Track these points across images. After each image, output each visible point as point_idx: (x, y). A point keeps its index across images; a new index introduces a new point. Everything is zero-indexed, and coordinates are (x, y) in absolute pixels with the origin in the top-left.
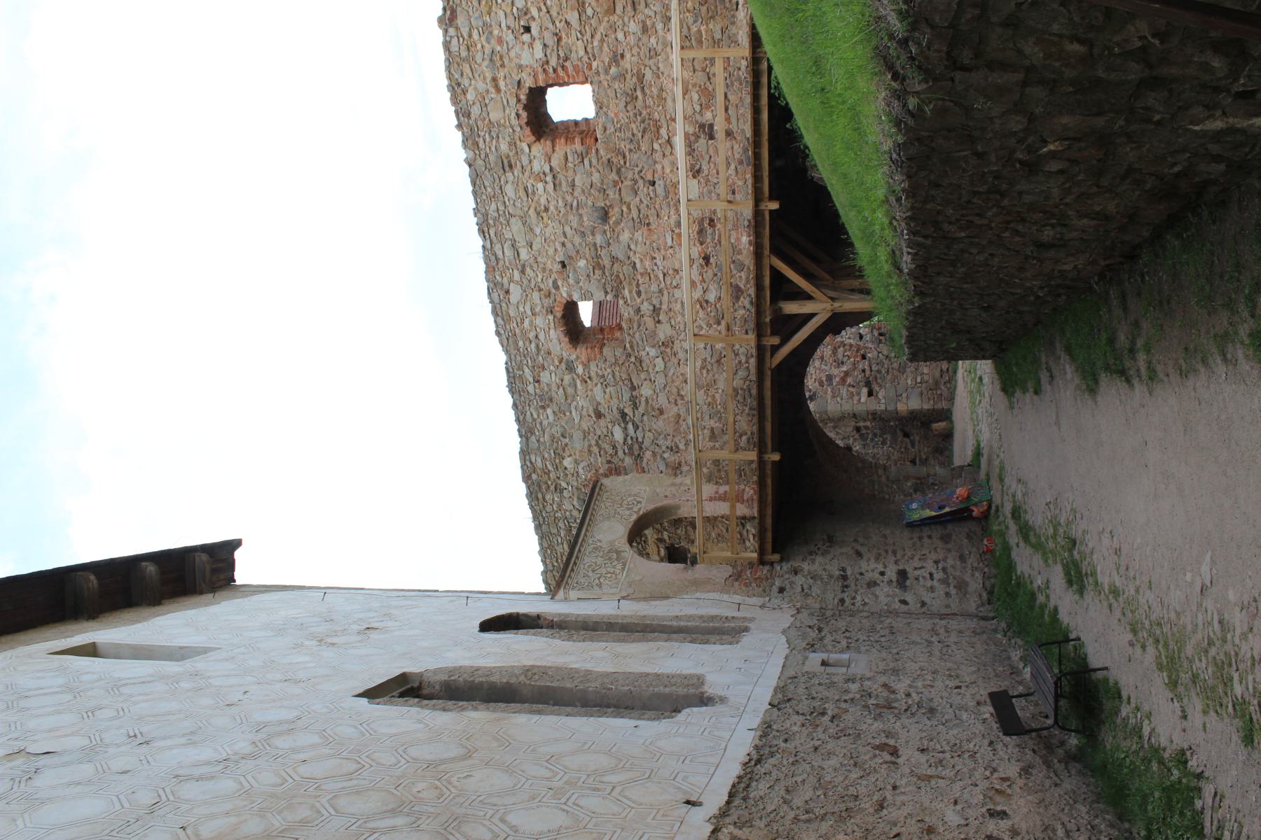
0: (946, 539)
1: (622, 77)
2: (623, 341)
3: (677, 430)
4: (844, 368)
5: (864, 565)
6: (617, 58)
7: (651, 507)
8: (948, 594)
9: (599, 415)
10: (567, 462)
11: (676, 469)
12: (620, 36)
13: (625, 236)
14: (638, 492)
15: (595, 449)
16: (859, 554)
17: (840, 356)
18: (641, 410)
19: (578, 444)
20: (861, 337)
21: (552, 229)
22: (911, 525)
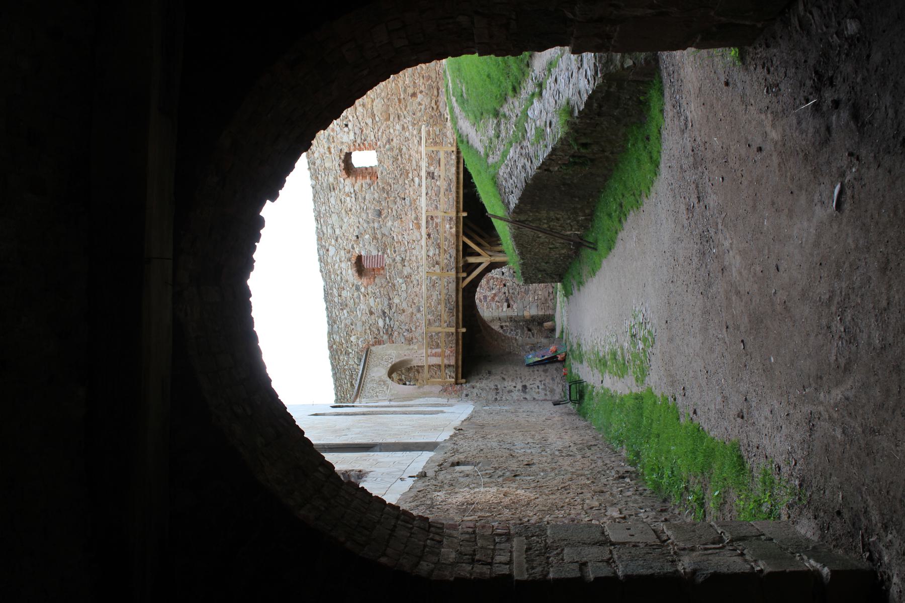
0: (545, 371)
1: (392, 149)
2: (385, 275)
3: (411, 320)
4: (494, 292)
5: (506, 384)
6: (389, 141)
7: (398, 360)
8: (546, 395)
9: (371, 313)
10: (353, 339)
11: (410, 341)
12: (392, 131)
13: (390, 223)
14: (390, 353)
15: (368, 331)
16: (504, 379)
17: (491, 285)
18: (393, 310)
19: (359, 328)
20: (503, 274)
21: (353, 219)
22: (529, 365)
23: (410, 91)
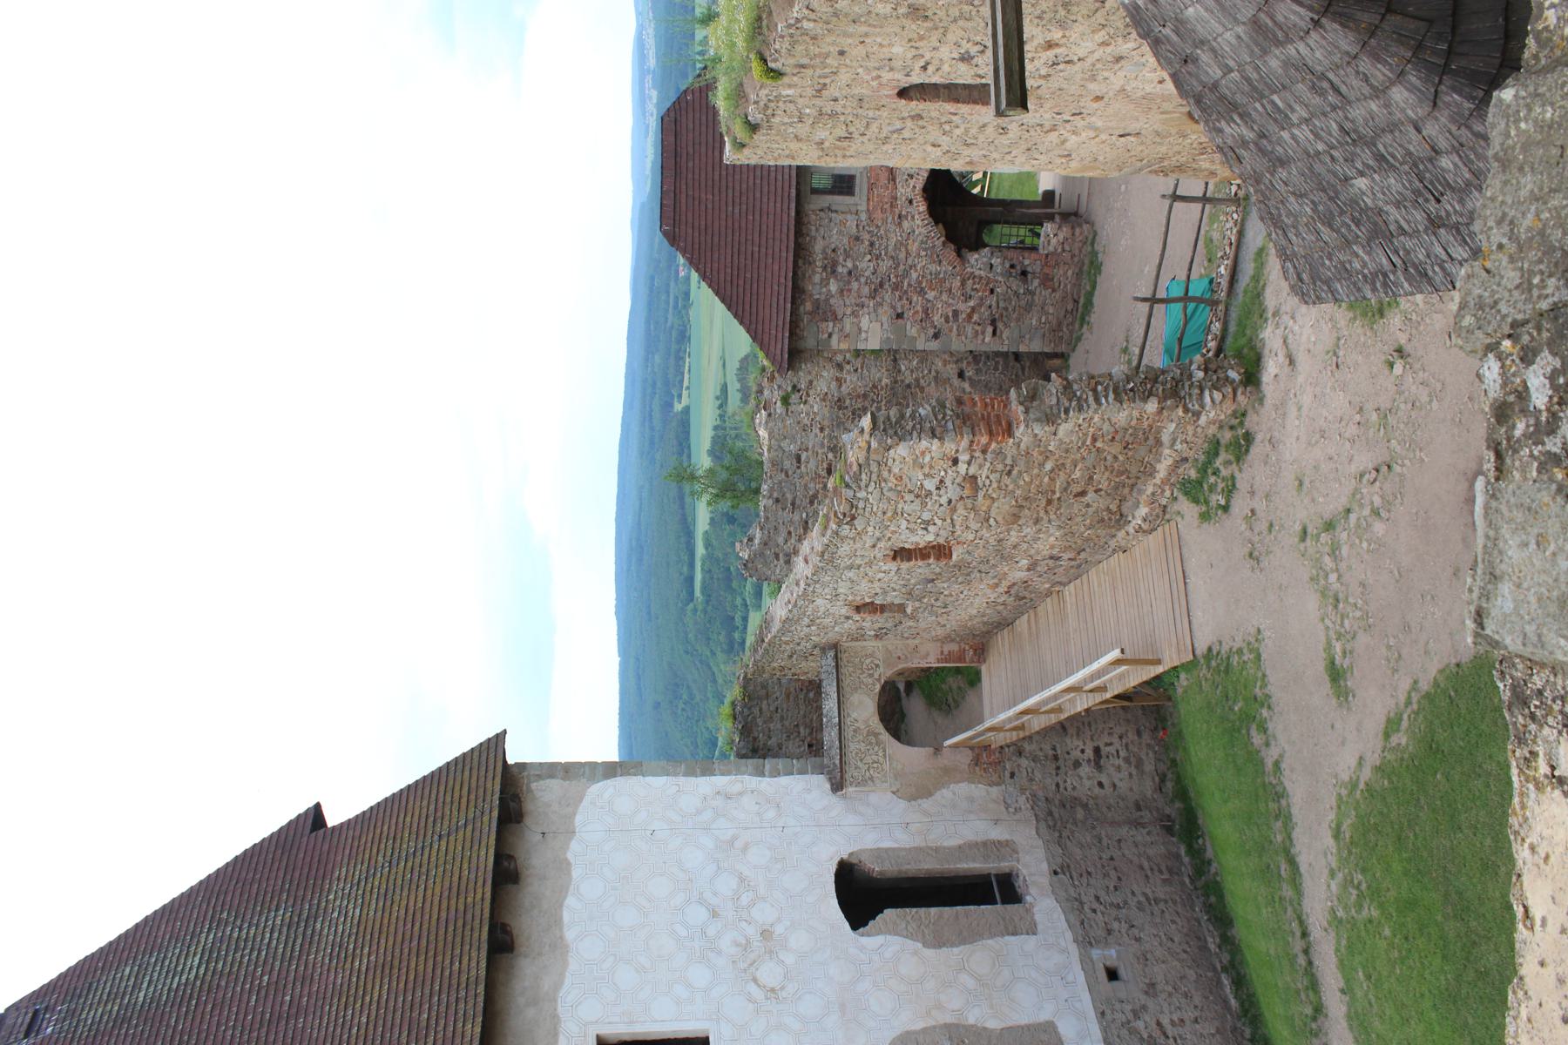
4: (972, 303)
23: (1076, 489)
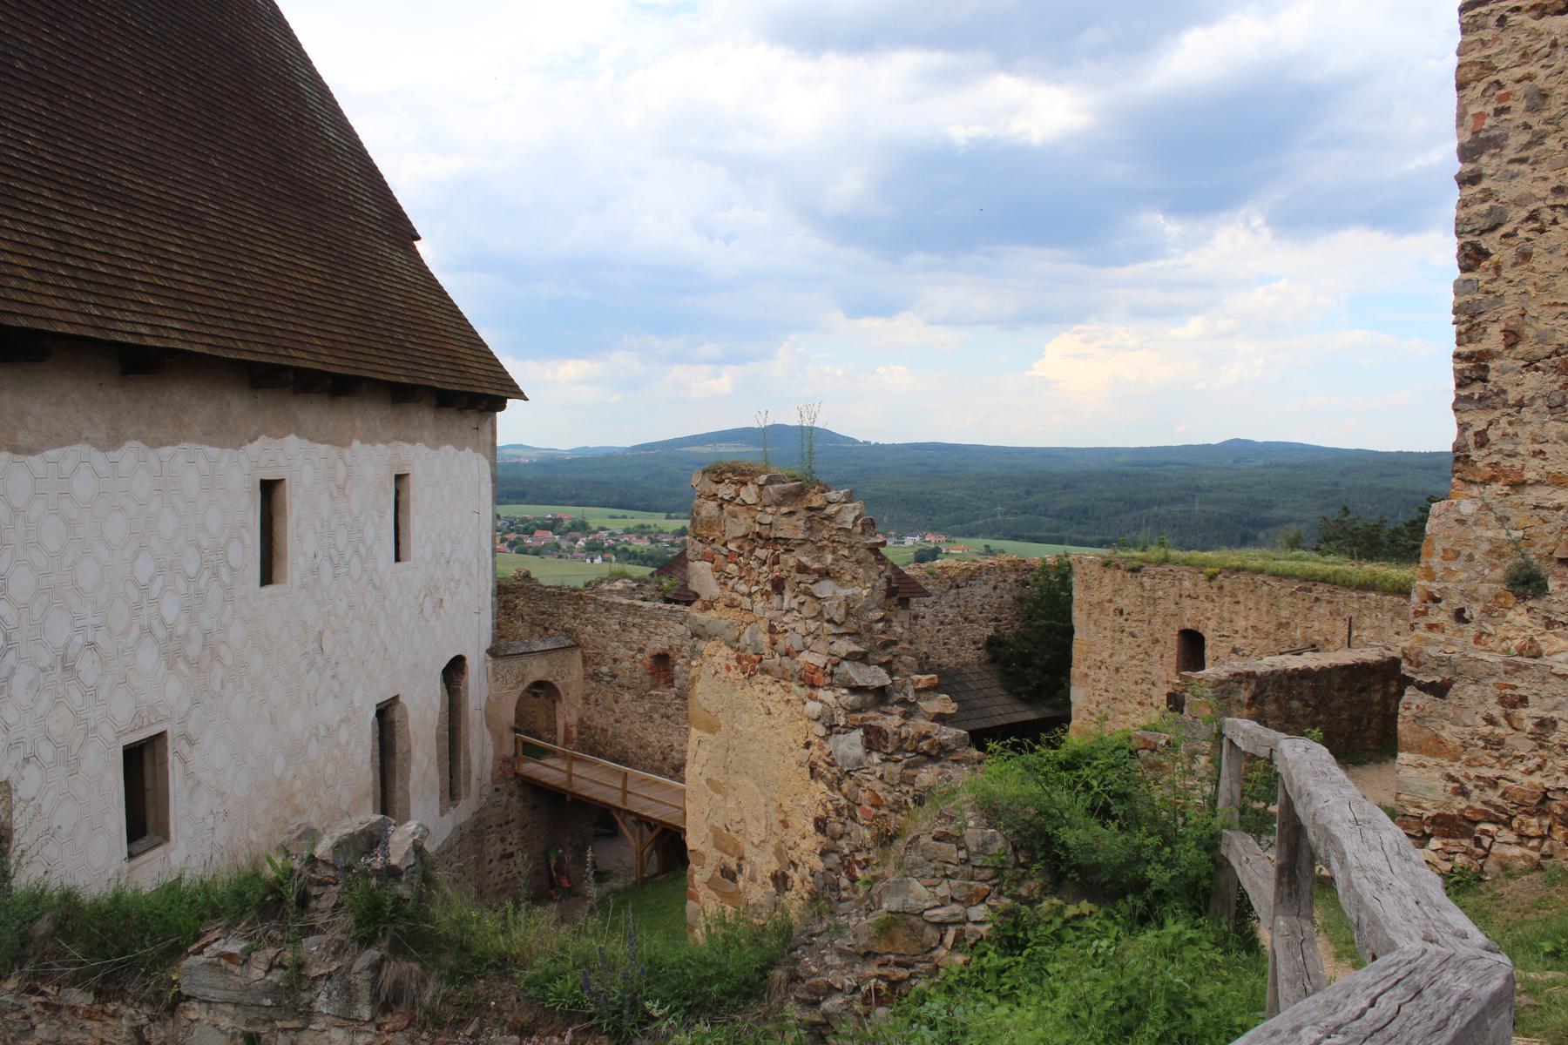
0: (537, 873)
2: (655, 687)
11: (586, 699)
14: (571, 676)
